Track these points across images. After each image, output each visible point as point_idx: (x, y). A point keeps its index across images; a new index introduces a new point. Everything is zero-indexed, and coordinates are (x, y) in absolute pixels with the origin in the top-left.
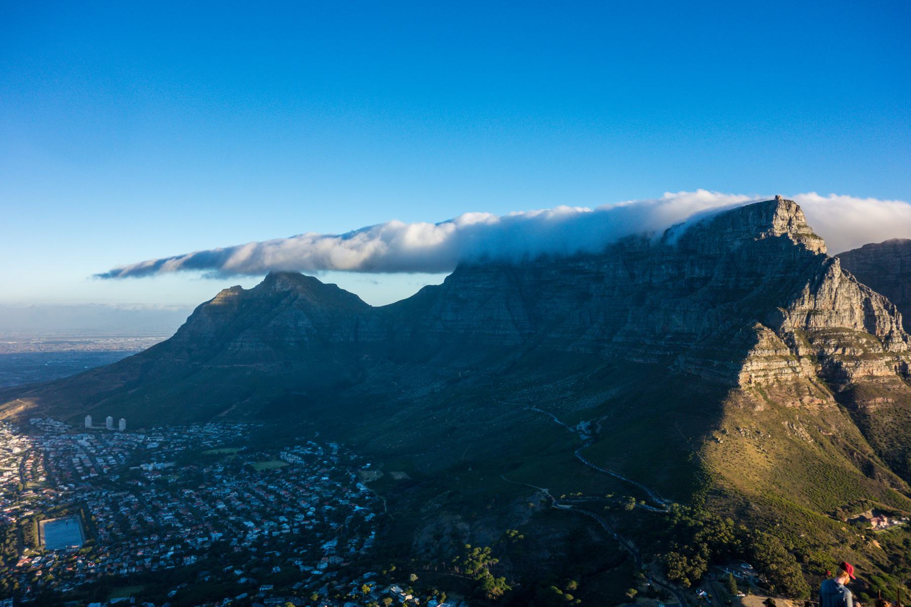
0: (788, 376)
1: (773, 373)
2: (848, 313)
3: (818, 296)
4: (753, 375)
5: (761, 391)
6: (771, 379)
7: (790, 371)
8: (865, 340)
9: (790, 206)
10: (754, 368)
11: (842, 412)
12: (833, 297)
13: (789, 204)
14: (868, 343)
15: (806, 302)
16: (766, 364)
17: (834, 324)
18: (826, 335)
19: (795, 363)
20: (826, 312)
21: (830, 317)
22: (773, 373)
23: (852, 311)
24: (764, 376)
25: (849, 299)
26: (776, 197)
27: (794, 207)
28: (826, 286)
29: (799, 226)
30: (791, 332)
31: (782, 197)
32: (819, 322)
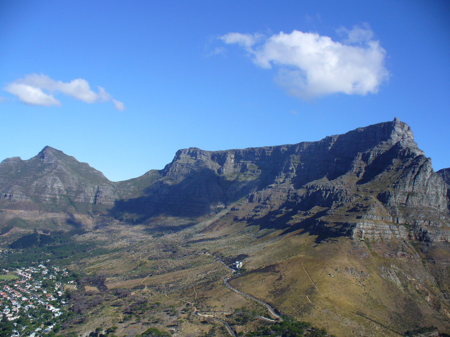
0: (389, 236)
1: (378, 232)
2: (434, 198)
3: (415, 183)
4: (364, 232)
5: (368, 244)
6: (377, 237)
7: (391, 232)
8: (444, 218)
9: (403, 126)
10: (365, 227)
11: (425, 266)
12: (425, 184)
13: (403, 125)
14: (446, 219)
15: (407, 187)
16: (374, 225)
17: (425, 204)
18: (419, 210)
19: (395, 228)
20: (419, 195)
21: (423, 199)
22: (378, 232)
23: (438, 197)
24: (372, 233)
25: (437, 187)
26: (395, 119)
27: (406, 128)
28: (420, 177)
29: (409, 141)
30: (394, 207)
31: (398, 120)
32: (414, 201)
